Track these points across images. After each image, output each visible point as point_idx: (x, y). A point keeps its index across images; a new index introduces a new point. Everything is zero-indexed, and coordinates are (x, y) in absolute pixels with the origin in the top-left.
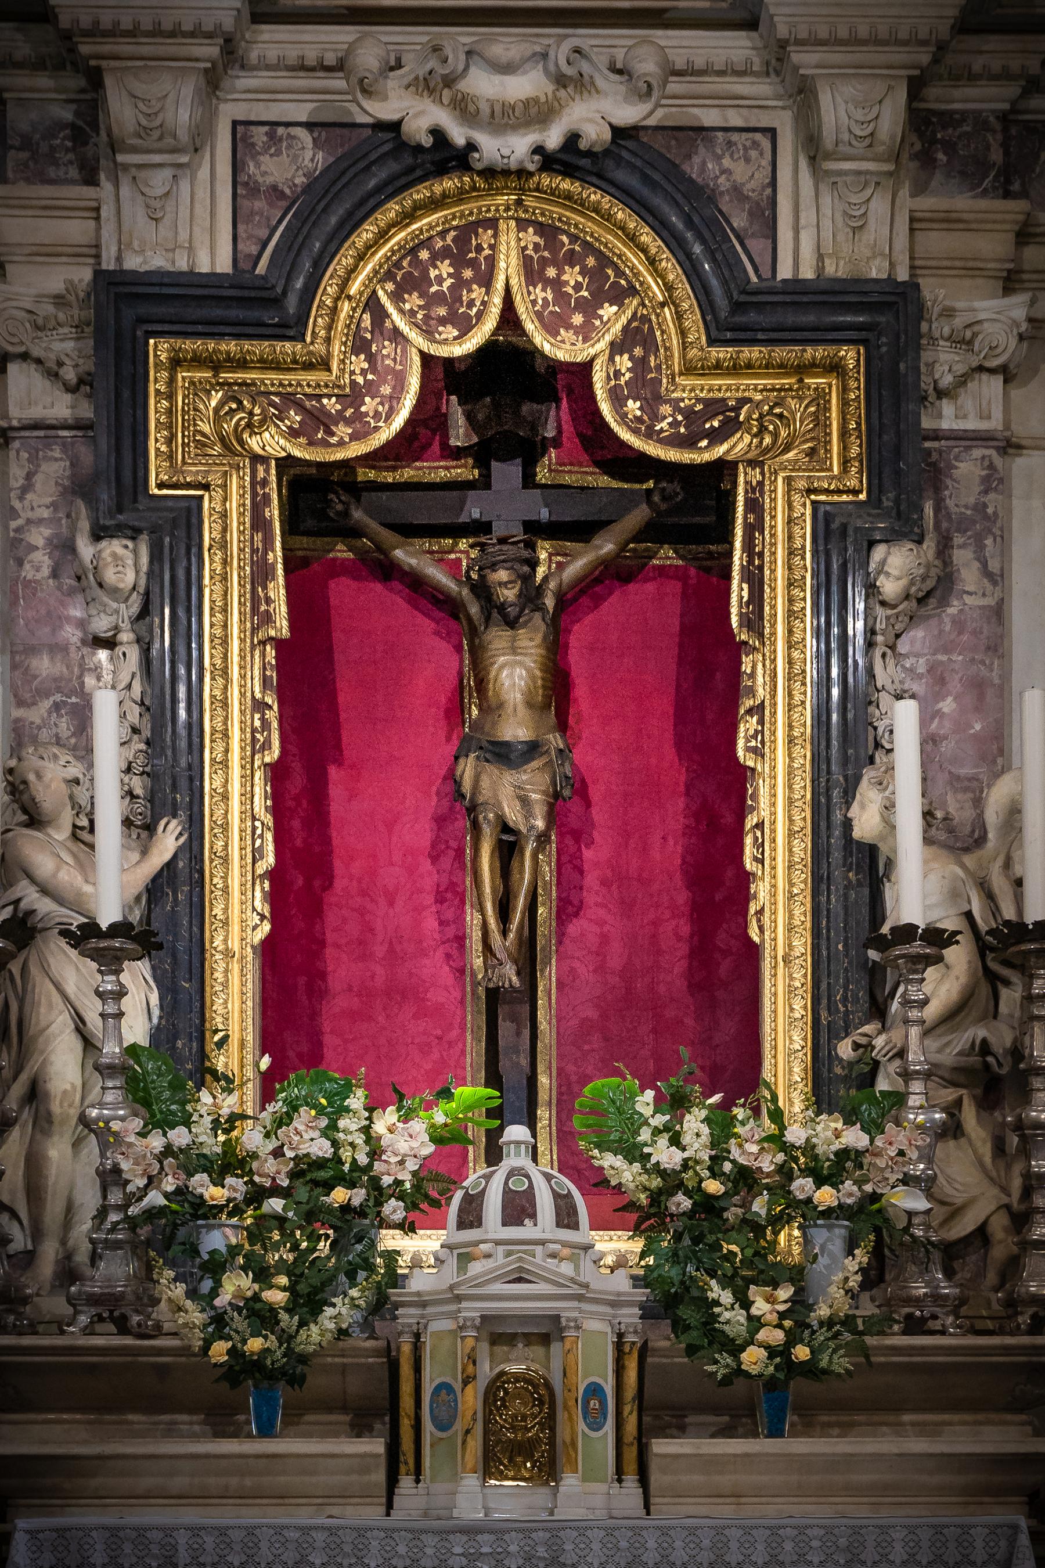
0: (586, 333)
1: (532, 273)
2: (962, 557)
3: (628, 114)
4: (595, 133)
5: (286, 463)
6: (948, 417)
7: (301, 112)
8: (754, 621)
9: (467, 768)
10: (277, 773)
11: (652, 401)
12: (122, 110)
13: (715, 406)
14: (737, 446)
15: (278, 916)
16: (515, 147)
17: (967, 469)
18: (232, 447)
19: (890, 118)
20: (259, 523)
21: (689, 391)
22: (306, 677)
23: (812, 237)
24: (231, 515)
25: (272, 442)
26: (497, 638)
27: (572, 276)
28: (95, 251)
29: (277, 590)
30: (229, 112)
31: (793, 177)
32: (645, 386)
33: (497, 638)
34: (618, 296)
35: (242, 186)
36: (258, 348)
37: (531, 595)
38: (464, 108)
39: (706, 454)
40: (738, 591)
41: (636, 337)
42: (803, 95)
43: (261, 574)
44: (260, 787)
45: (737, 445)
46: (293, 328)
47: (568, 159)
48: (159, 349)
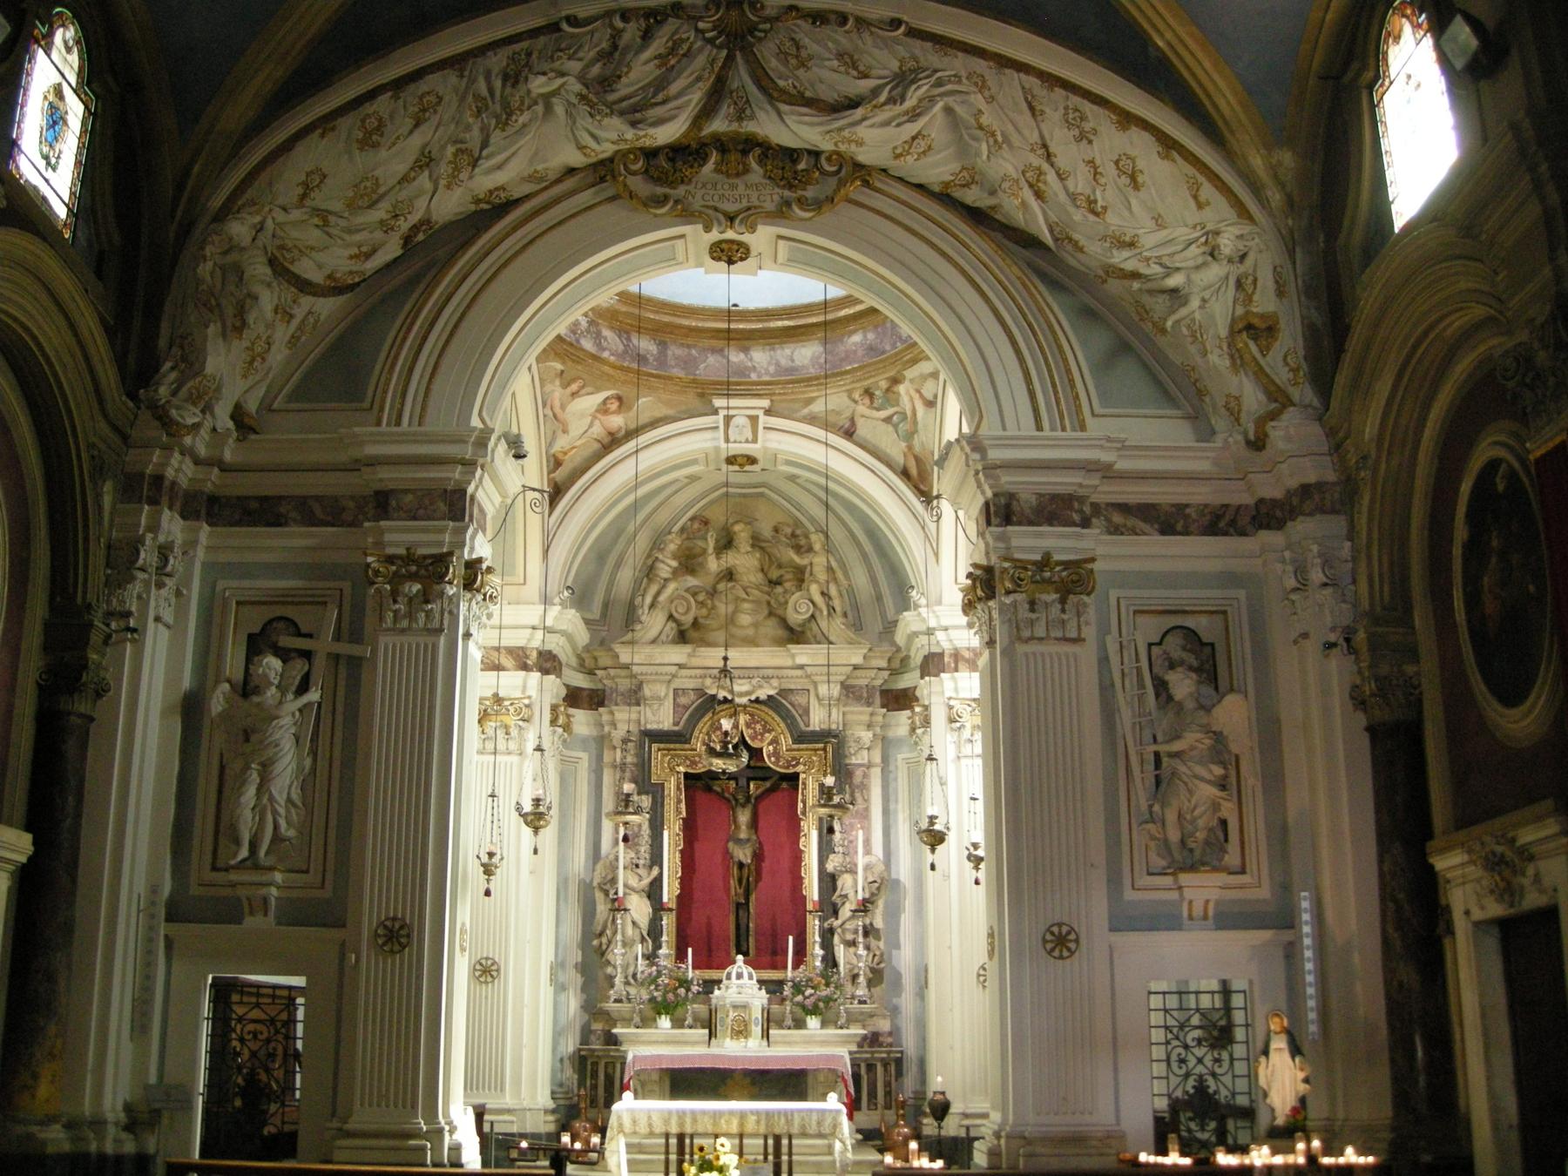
0: (762, 741)
1: (748, 725)
2: (858, 795)
3: (772, 692)
4: (763, 697)
5: (686, 774)
6: (854, 761)
7: (691, 686)
8: (804, 813)
9: (731, 845)
10: (682, 852)
11: (778, 759)
12: (647, 691)
13: (794, 758)
14: (800, 768)
15: (682, 889)
16: (744, 700)
17: (859, 773)
18: (672, 769)
19: (836, 690)
20: (679, 789)
21: (788, 756)
22: (690, 828)
23: (817, 719)
24: (673, 788)
25: (682, 769)
26: (739, 811)
27: (758, 727)
28: (639, 722)
29: (683, 806)
30: (673, 686)
31: (813, 701)
32: (776, 754)
33: (739, 811)
34: (769, 731)
35: (676, 705)
36: (678, 746)
37: (748, 799)
38: (732, 692)
39: (791, 770)
40: (800, 805)
41: (775, 741)
42: (815, 684)
43: (679, 801)
44: (678, 855)
45: (800, 768)
46: (688, 741)
47: (757, 701)
48: (655, 746)
